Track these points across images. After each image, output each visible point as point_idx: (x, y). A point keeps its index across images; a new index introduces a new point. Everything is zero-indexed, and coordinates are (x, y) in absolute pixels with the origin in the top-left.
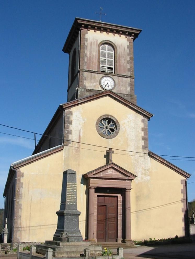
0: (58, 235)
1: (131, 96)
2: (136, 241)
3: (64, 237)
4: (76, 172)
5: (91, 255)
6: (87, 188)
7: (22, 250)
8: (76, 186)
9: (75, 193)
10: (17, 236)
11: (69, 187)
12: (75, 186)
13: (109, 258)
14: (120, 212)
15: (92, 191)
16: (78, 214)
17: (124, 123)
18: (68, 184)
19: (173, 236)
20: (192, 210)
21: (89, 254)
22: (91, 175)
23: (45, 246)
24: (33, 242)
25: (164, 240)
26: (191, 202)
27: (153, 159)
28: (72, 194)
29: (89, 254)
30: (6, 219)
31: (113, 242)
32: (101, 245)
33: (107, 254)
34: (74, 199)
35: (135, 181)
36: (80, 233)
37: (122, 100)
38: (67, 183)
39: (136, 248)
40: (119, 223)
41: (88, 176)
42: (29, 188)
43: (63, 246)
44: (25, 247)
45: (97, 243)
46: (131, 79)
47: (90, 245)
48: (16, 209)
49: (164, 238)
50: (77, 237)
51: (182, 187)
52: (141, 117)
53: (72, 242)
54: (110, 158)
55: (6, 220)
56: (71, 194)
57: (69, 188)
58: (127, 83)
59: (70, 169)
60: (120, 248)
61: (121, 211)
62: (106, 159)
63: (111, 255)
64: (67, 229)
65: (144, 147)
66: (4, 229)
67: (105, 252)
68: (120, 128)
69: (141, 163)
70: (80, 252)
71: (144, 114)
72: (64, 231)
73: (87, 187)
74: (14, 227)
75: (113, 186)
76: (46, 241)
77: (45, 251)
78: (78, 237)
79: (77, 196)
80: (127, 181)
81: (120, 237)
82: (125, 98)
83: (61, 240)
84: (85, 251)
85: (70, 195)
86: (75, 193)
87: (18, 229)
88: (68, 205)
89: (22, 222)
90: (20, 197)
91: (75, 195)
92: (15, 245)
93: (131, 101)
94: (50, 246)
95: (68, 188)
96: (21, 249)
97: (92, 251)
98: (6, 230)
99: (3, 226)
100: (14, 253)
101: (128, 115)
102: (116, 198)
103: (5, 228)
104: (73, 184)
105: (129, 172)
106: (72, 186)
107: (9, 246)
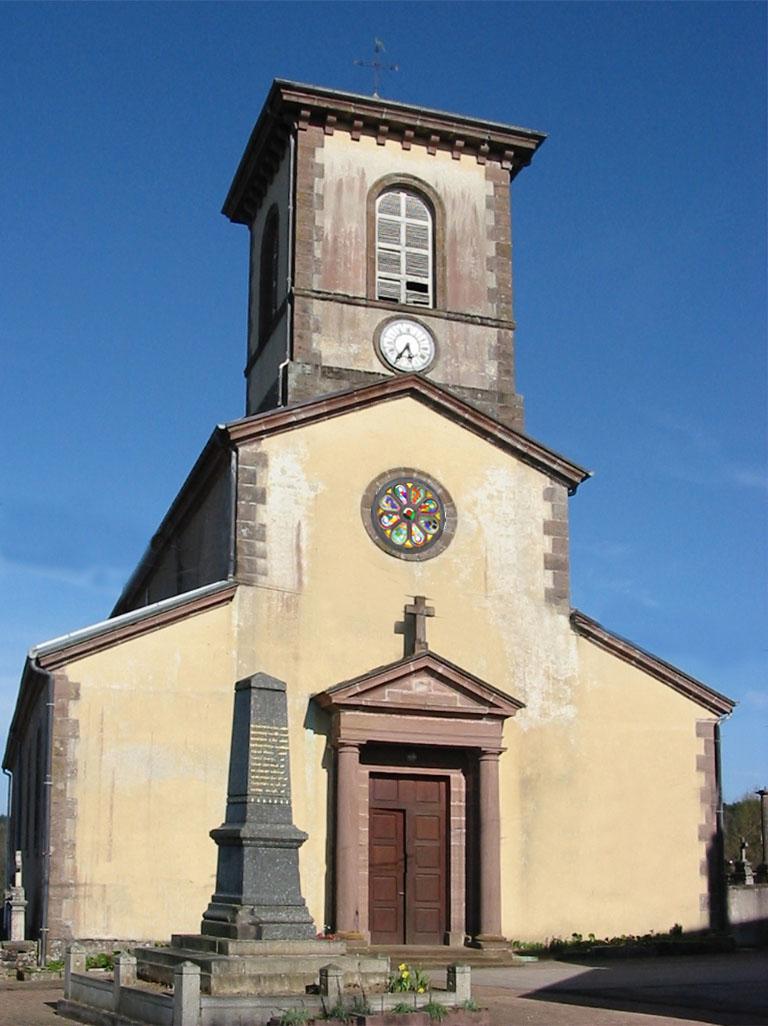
0: (218, 913)
1: (502, 396)
2: (522, 941)
3: (244, 922)
4: (285, 684)
5: (347, 990)
6: (329, 747)
7: (84, 968)
8: (286, 738)
9: (283, 763)
10: (63, 916)
11: (258, 739)
12: (281, 738)
13: (417, 1001)
14: (461, 821)
15: (350, 757)
16: (296, 840)
17: (475, 503)
18: (255, 729)
19: (665, 928)
20: (739, 831)
21: (338, 986)
22: (345, 697)
23: (170, 953)
24: (125, 939)
25: (630, 940)
26: (734, 804)
27: (590, 641)
28: (272, 765)
29: (342, 986)
30: (18, 853)
31: (433, 942)
32: (385, 954)
33: (408, 987)
34: (279, 785)
35: (517, 722)
36: (306, 911)
37: (466, 411)
38: (252, 726)
39: (519, 966)
40: (453, 876)
41: (334, 701)
42: (101, 740)
43: (241, 955)
44: (94, 956)
45: (369, 946)
46: (503, 331)
47: (343, 955)
48: (53, 818)
49: (627, 935)
50: (294, 925)
51: (699, 747)
52: (539, 481)
53: (275, 942)
54: (419, 635)
55: (18, 858)
56: (266, 765)
57: (259, 742)
58: (487, 349)
59: (260, 673)
60: (461, 966)
61: (460, 816)
62: (402, 636)
63: (425, 991)
64: (254, 896)
65: (555, 597)
66: (9, 889)
67: (400, 981)
68: (459, 524)
69: (542, 654)
70: (304, 977)
71: (555, 467)
72: (243, 900)
73: (327, 740)
74: (48, 883)
75: (429, 738)
76: (173, 936)
77: (172, 971)
78: (299, 923)
79: (289, 774)
80: (483, 722)
81: (460, 928)
82: (477, 404)
83: (230, 932)
84: (327, 976)
85: (262, 771)
86: (283, 763)
87: (66, 890)
88: (258, 807)
89: (78, 865)
90: (69, 775)
91: (282, 770)
92: (56, 948)
93: (503, 417)
94: (188, 953)
95: (254, 742)
96: (77, 964)
97: (352, 974)
98: (18, 894)
99: (6, 879)
100: (53, 978)
101: (488, 472)
102: (443, 784)
103: (14, 885)
104: (276, 731)
105: (492, 690)
106: (268, 737)
107: (33, 953)
